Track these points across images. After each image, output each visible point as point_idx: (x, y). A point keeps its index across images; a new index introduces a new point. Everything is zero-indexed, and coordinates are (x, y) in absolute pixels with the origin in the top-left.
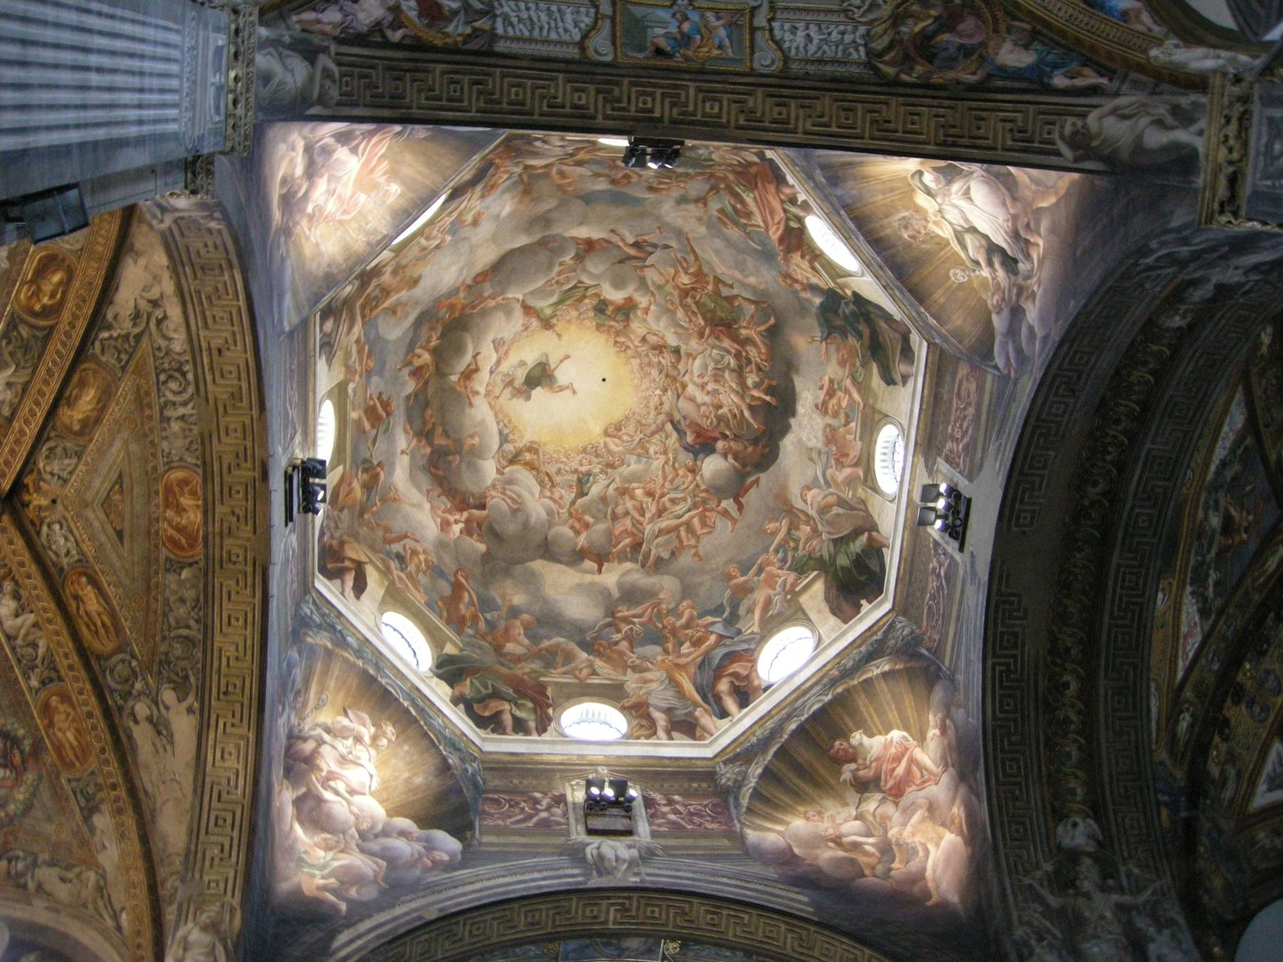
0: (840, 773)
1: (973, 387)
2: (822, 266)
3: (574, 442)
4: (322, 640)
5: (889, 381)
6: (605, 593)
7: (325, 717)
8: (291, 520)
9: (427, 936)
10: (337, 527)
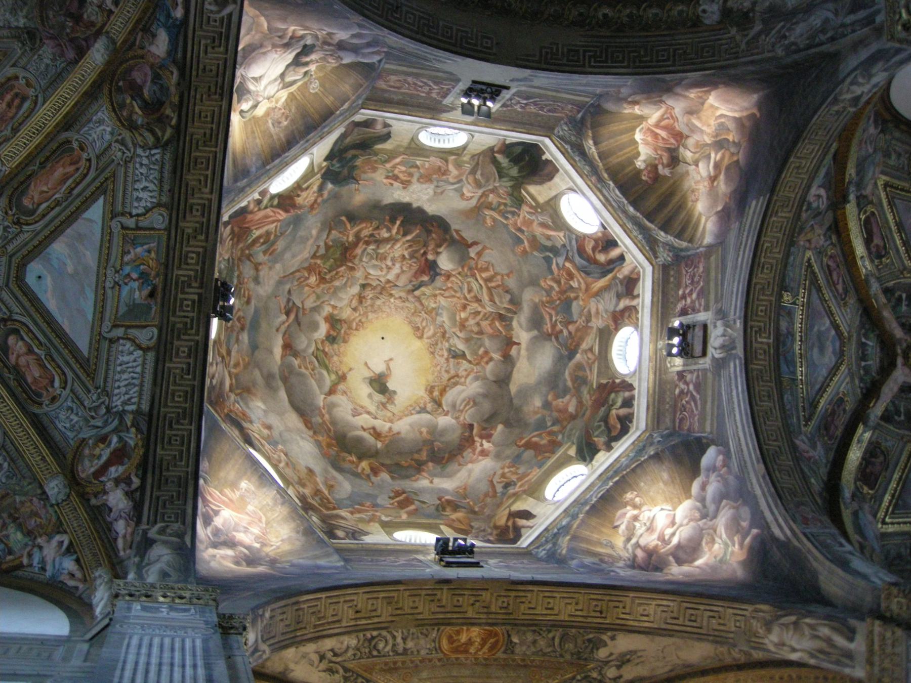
0: (665, 176)
1: (393, 78)
2: (306, 182)
3: (427, 360)
4: (564, 542)
5: (388, 136)
6: (534, 341)
7: (619, 542)
8: (478, 563)
9: (777, 472)
10: (484, 530)
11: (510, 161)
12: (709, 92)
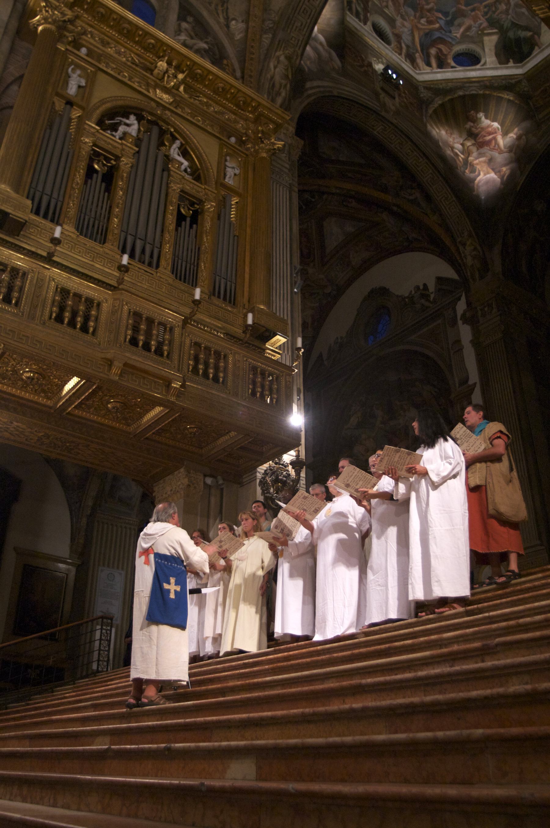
11: (520, 37)
12: (502, 178)
